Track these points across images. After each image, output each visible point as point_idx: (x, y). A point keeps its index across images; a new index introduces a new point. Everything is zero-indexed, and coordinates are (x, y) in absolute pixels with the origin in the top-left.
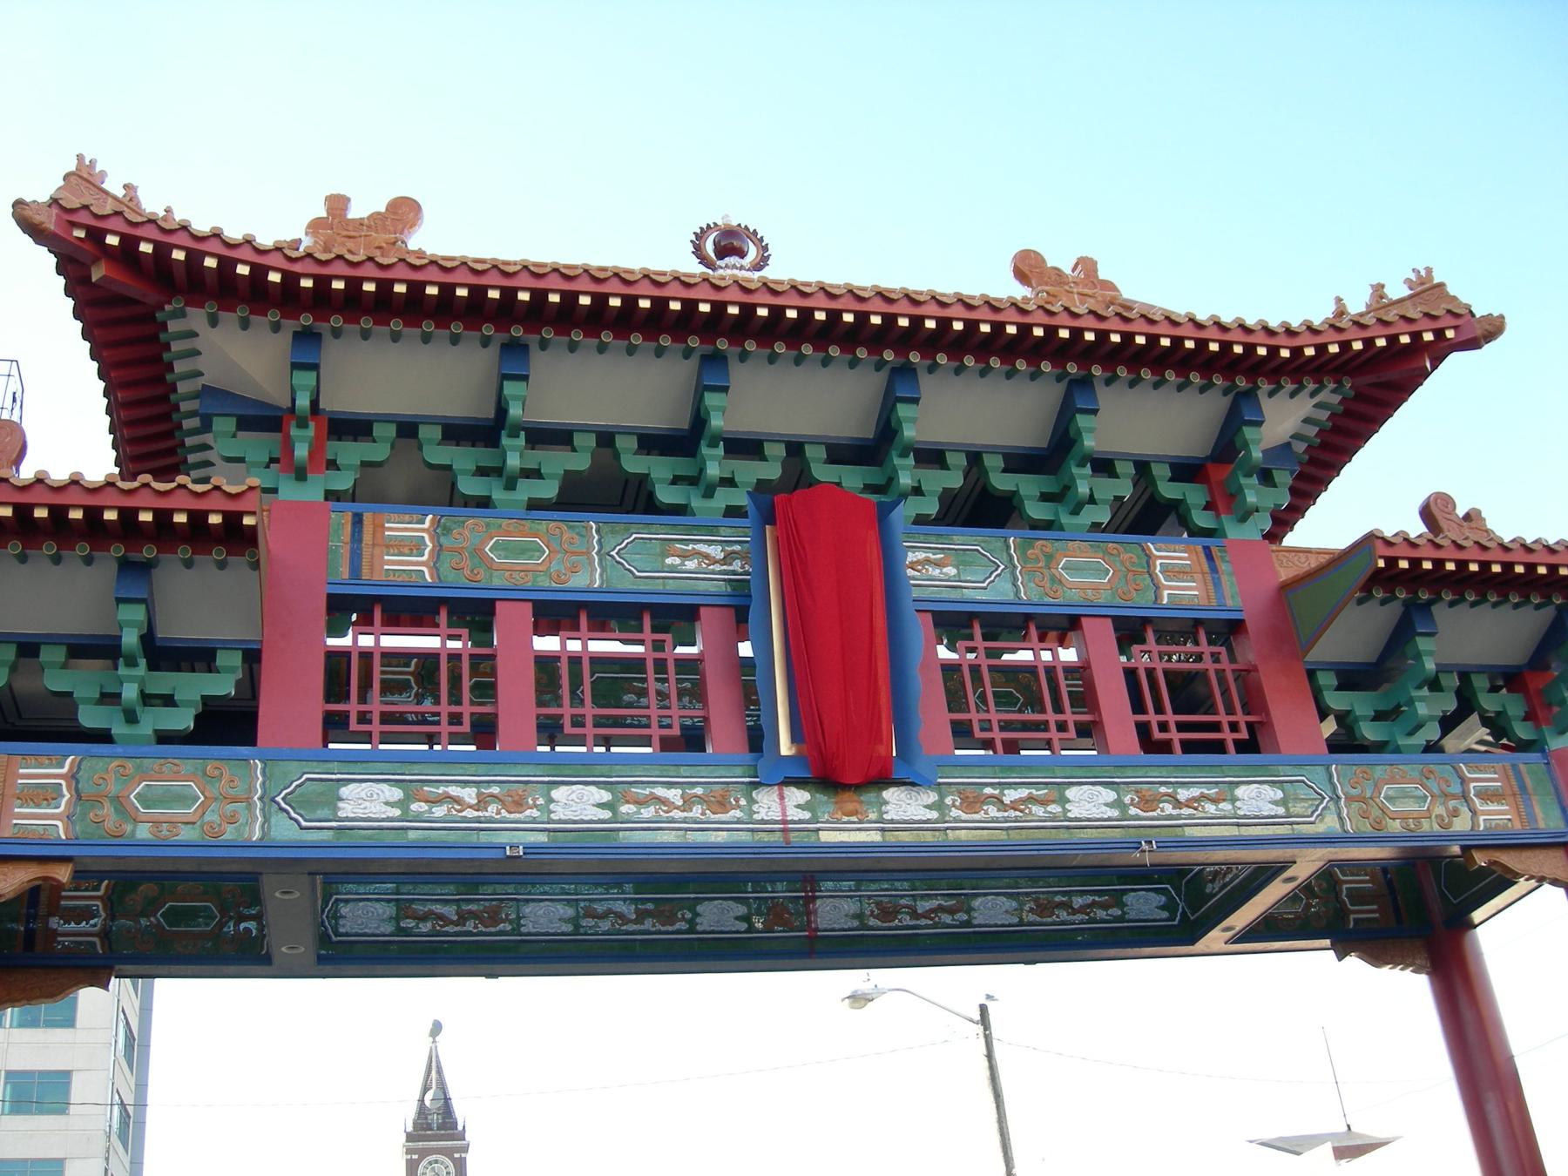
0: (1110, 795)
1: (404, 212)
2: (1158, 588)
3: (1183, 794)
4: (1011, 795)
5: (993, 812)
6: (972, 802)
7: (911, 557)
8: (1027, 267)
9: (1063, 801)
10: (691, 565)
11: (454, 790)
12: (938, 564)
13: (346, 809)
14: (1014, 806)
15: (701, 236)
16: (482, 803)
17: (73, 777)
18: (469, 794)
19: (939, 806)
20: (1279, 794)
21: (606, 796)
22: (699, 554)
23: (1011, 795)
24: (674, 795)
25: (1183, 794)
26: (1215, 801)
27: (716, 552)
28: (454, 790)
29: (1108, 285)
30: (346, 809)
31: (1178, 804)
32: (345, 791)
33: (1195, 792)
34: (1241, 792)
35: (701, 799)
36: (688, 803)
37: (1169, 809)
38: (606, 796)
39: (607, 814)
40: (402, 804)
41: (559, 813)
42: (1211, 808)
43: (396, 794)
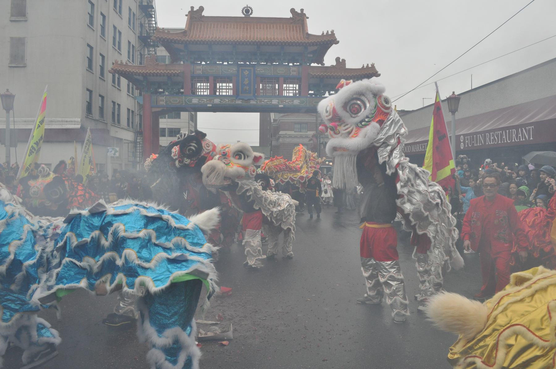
0: (277, 101)
1: (201, 9)
2: (290, 73)
3: (287, 101)
4: (265, 101)
5: (263, 103)
6: (261, 101)
7: (258, 69)
8: (293, 11)
9: (271, 101)
10: (232, 71)
11: (204, 100)
12: (262, 71)
13: (193, 102)
14: (265, 102)
15: (243, 10)
16: (207, 101)
17: (165, 98)
18: (205, 100)
19: (257, 102)
20: (299, 101)
21: (220, 100)
22: (232, 70)
23: (265, 101)
24: (227, 100)
25: (287, 101)
26: (291, 102)
27: (235, 69)
28: (204, 100)
29: (305, 14)
30: (193, 102)
31: (286, 102)
32: (193, 100)
33: (288, 101)
34: (294, 101)
35: (230, 101)
36: (229, 101)
37: (284, 103)
38: (220, 100)
39: (220, 102)
40: (198, 101)
41: (215, 102)
42: (290, 103)
43: (198, 100)
